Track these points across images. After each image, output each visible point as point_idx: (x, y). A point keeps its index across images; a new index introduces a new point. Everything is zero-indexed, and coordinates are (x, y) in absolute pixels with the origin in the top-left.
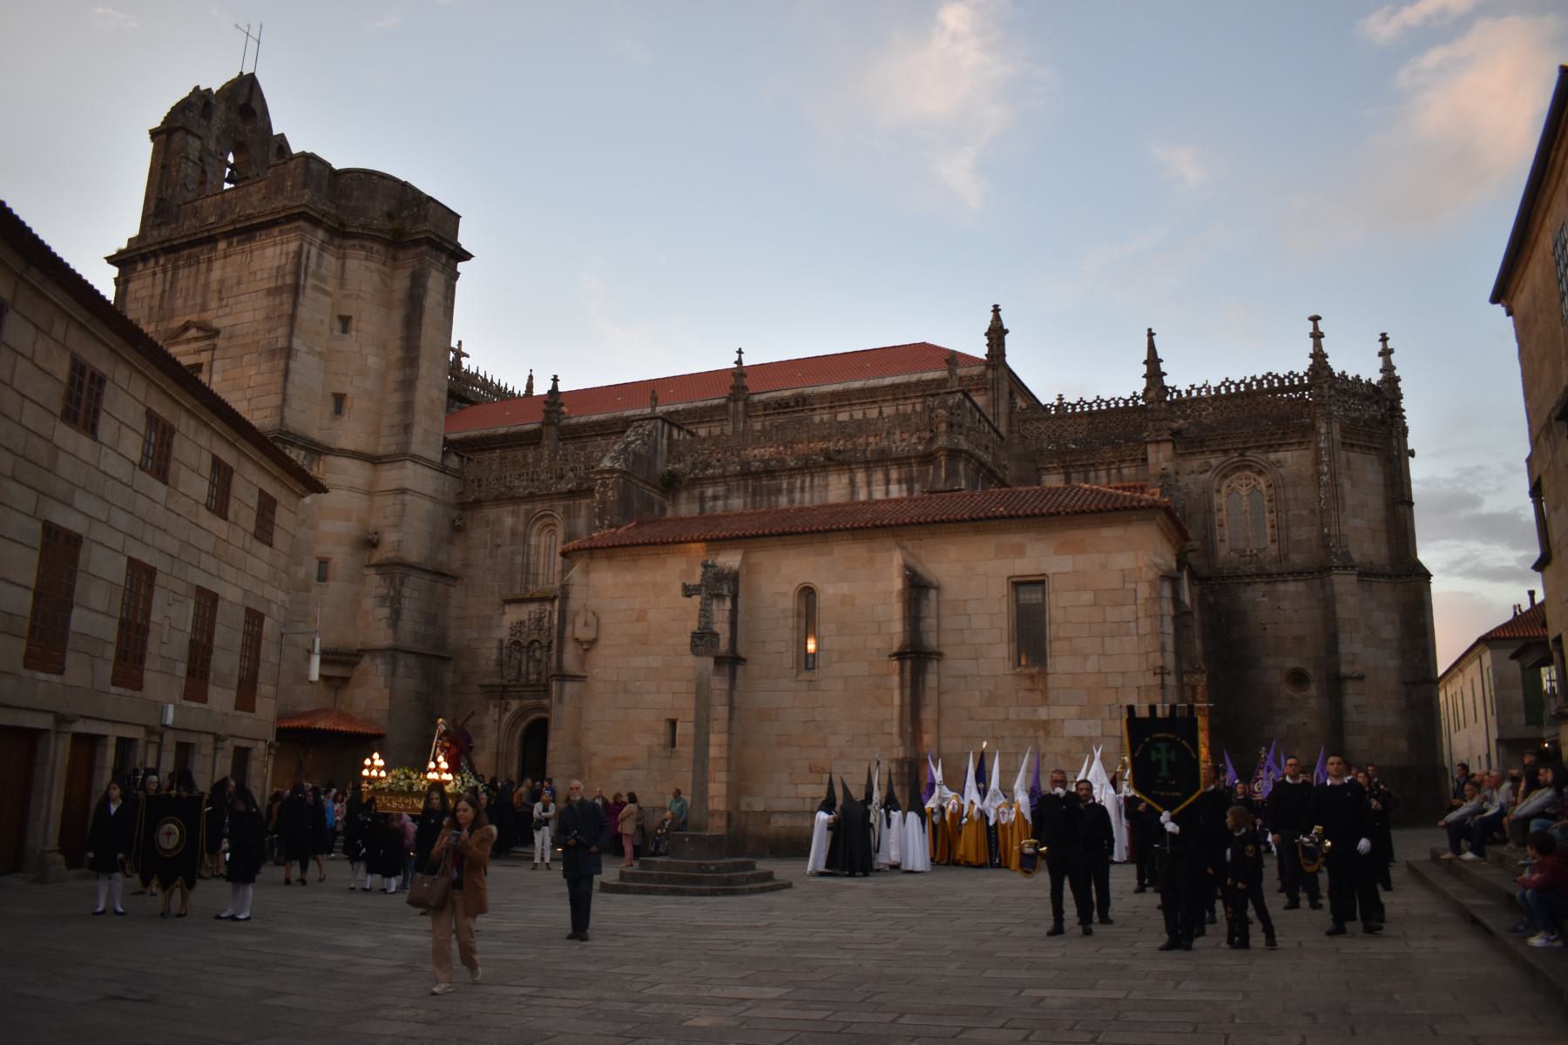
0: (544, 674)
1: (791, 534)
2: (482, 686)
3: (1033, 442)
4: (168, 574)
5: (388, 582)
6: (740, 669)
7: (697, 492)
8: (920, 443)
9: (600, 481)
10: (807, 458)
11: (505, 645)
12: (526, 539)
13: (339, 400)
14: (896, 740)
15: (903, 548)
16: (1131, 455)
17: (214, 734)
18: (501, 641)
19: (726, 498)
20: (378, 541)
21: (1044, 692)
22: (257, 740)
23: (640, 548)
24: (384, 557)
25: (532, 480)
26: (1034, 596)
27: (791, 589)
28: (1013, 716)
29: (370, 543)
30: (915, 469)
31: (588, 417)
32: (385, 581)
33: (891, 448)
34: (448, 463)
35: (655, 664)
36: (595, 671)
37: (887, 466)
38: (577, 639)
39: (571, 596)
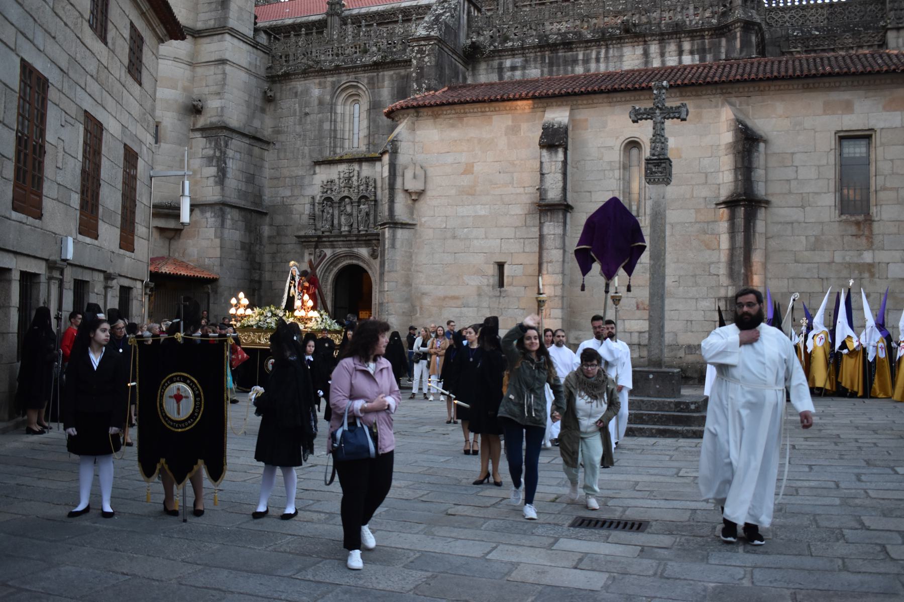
0: (355, 225)
1: (622, 90)
2: (298, 237)
3: (778, 29)
4: (59, 90)
5: (213, 143)
7: (495, 63)
8: (713, 17)
9: (416, 48)
10: (603, 32)
11: (317, 201)
12: (332, 108)
14: (724, 280)
15: (732, 104)
16: (869, 41)
17: (104, 272)
18: (313, 198)
19: (524, 68)
20: (202, 108)
21: (870, 238)
22: (136, 280)
23: (467, 106)
24: (208, 122)
25: (337, 55)
26: (858, 150)
27: (618, 144)
28: (838, 258)
29: (195, 109)
30: (707, 41)
31: (367, 9)
32: (210, 143)
33: (685, 22)
34: (258, 39)
35: (483, 213)
36: (423, 220)
37: (680, 38)
38: (407, 191)
39: (399, 151)
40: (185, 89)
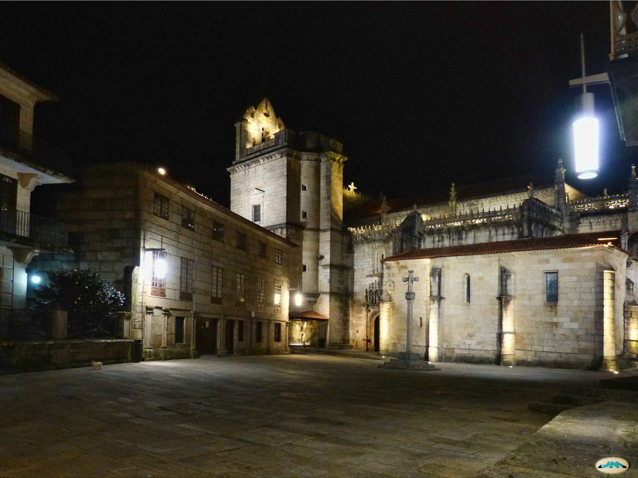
6: (442, 301)
18: (366, 290)
21: (556, 312)
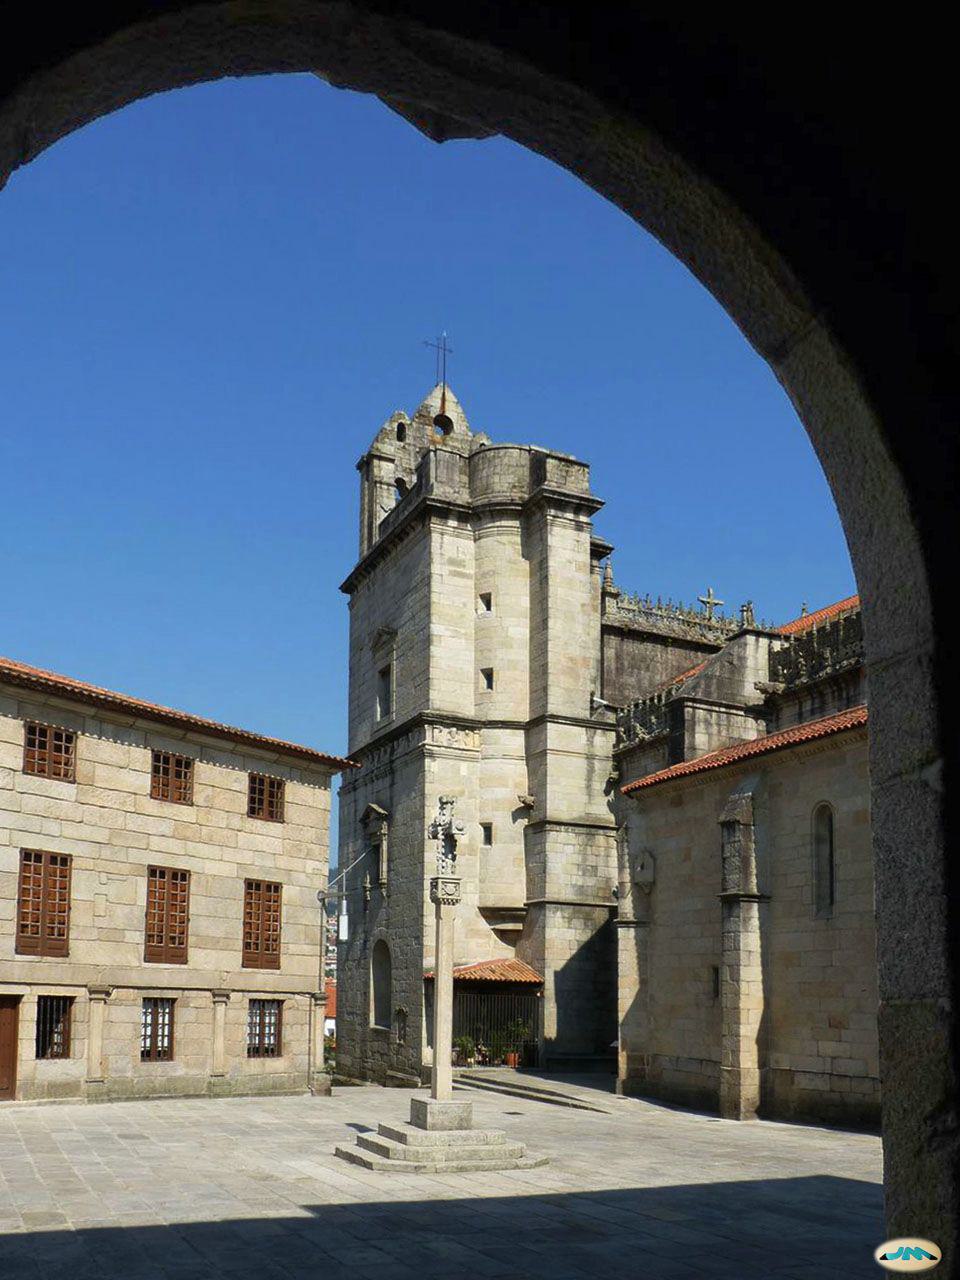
13: (489, 675)
40: (516, 786)
